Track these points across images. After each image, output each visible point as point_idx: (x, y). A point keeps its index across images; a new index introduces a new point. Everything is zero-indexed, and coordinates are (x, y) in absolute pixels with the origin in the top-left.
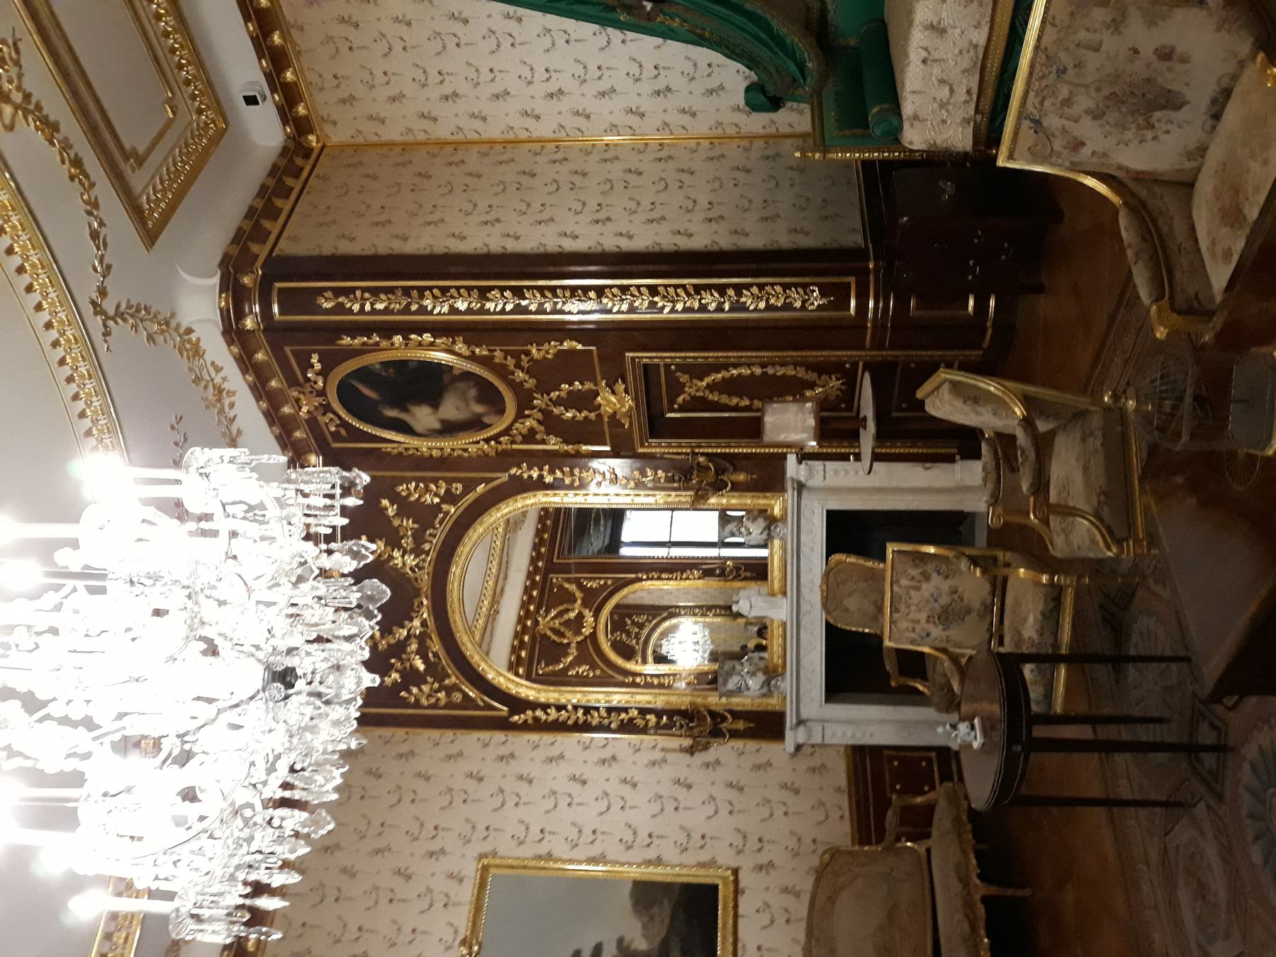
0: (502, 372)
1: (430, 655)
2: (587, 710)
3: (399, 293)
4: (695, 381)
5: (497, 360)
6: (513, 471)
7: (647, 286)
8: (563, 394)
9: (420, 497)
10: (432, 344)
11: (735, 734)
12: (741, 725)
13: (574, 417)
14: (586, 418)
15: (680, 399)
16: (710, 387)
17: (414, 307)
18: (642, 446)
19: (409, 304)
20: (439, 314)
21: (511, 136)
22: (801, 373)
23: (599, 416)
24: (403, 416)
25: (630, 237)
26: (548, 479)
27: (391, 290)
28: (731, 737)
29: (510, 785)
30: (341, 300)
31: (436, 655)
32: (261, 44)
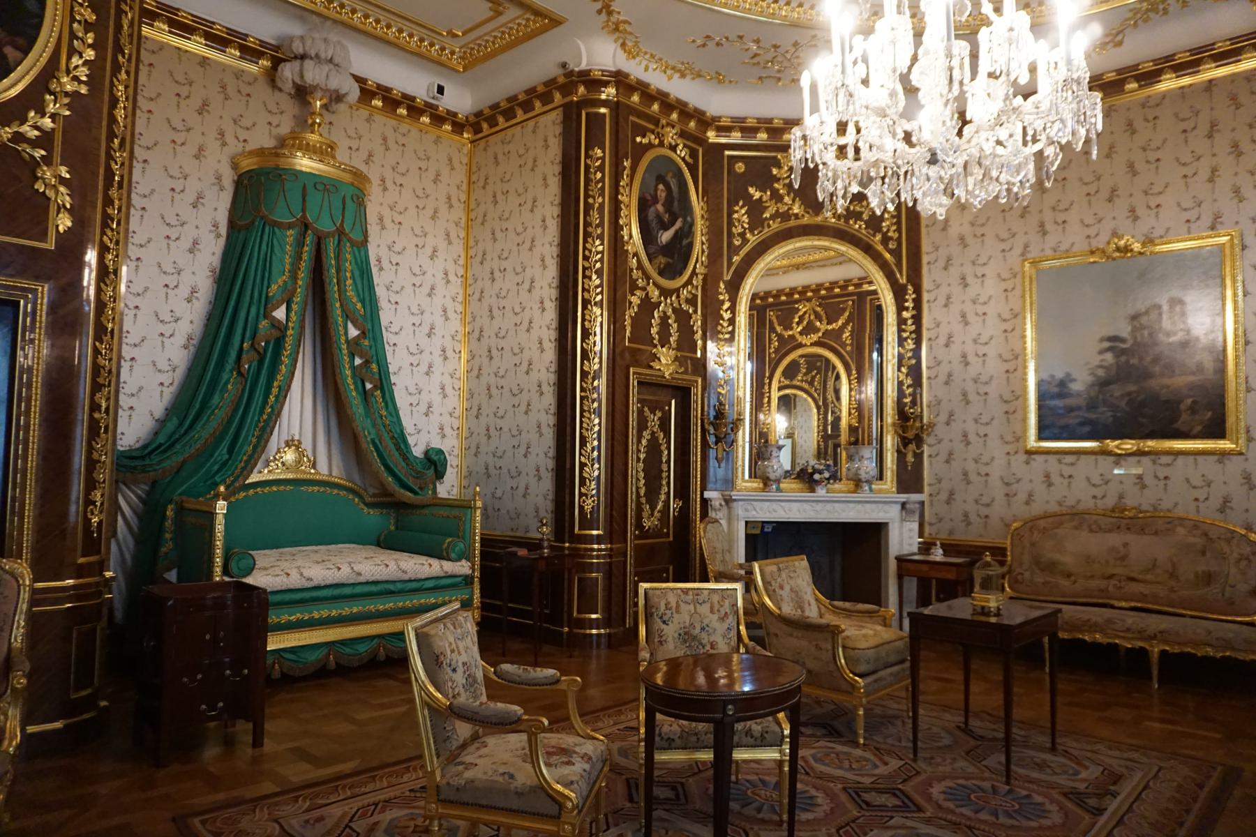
5: (32, 114)
32: (384, 92)
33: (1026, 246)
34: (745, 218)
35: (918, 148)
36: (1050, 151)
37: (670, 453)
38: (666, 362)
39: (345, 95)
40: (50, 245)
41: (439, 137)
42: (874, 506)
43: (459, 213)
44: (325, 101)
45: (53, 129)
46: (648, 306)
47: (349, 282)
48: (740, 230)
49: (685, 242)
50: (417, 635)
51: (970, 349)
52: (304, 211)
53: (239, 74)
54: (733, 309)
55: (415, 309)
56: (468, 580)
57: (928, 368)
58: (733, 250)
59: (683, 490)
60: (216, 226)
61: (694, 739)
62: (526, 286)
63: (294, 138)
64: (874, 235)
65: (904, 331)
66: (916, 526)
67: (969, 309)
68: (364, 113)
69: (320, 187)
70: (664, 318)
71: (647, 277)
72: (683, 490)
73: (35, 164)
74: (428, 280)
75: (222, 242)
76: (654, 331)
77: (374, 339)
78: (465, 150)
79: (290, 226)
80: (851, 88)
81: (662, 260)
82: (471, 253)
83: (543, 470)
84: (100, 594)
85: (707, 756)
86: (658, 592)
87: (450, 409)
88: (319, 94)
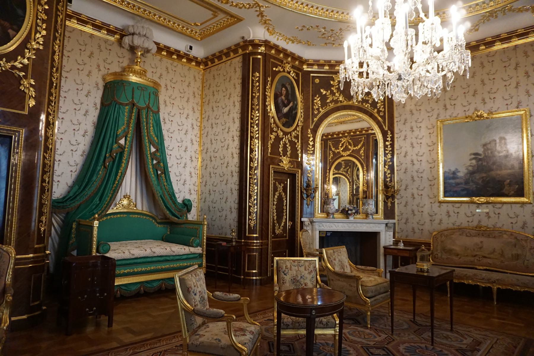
5: (19, 57)
20: (53, 45)
32: (167, 49)
33: (438, 115)
34: (319, 102)
35: (393, 73)
36: (449, 75)
37: (287, 202)
38: (285, 163)
39: (150, 50)
40: (26, 112)
41: (190, 67)
42: (374, 225)
43: (198, 99)
44: (142, 52)
45: (28, 64)
46: (278, 139)
47: (152, 128)
48: (317, 107)
49: (294, 112)
50: (180, 279)
51: (415, 158)
52: (133, 98)
53: (106, 41)
54: (314, 141)
55: (179, 140)
56: (201, 255)
57: (397, 166)
58: (314, 116)
59: (293, 217)
60: (95, 104)
61: (297, 325)
62: (227, 130)
63: (129, 68)
64: (374, 110)
65: (387, 150)
66: (392, 233)
67: (414, 141)
68: (159, 57)
69: (140, 88)
70: (285, 144)
71: (278, 127)
72: (293, 217)
73: (20, 78)
74: (185, 128)
75: (98, 111)
76: (280, 150)
77: (162, 154)
78: (201, 73)
79: (127, 105)
80: (365, 48)
81: (284, 120)
82: (203, 116)
83: (233, 210)
84: (44, 260)
85: (303, 332)
86: (282, 261)
87: (194, 182)
88: (140, 49)
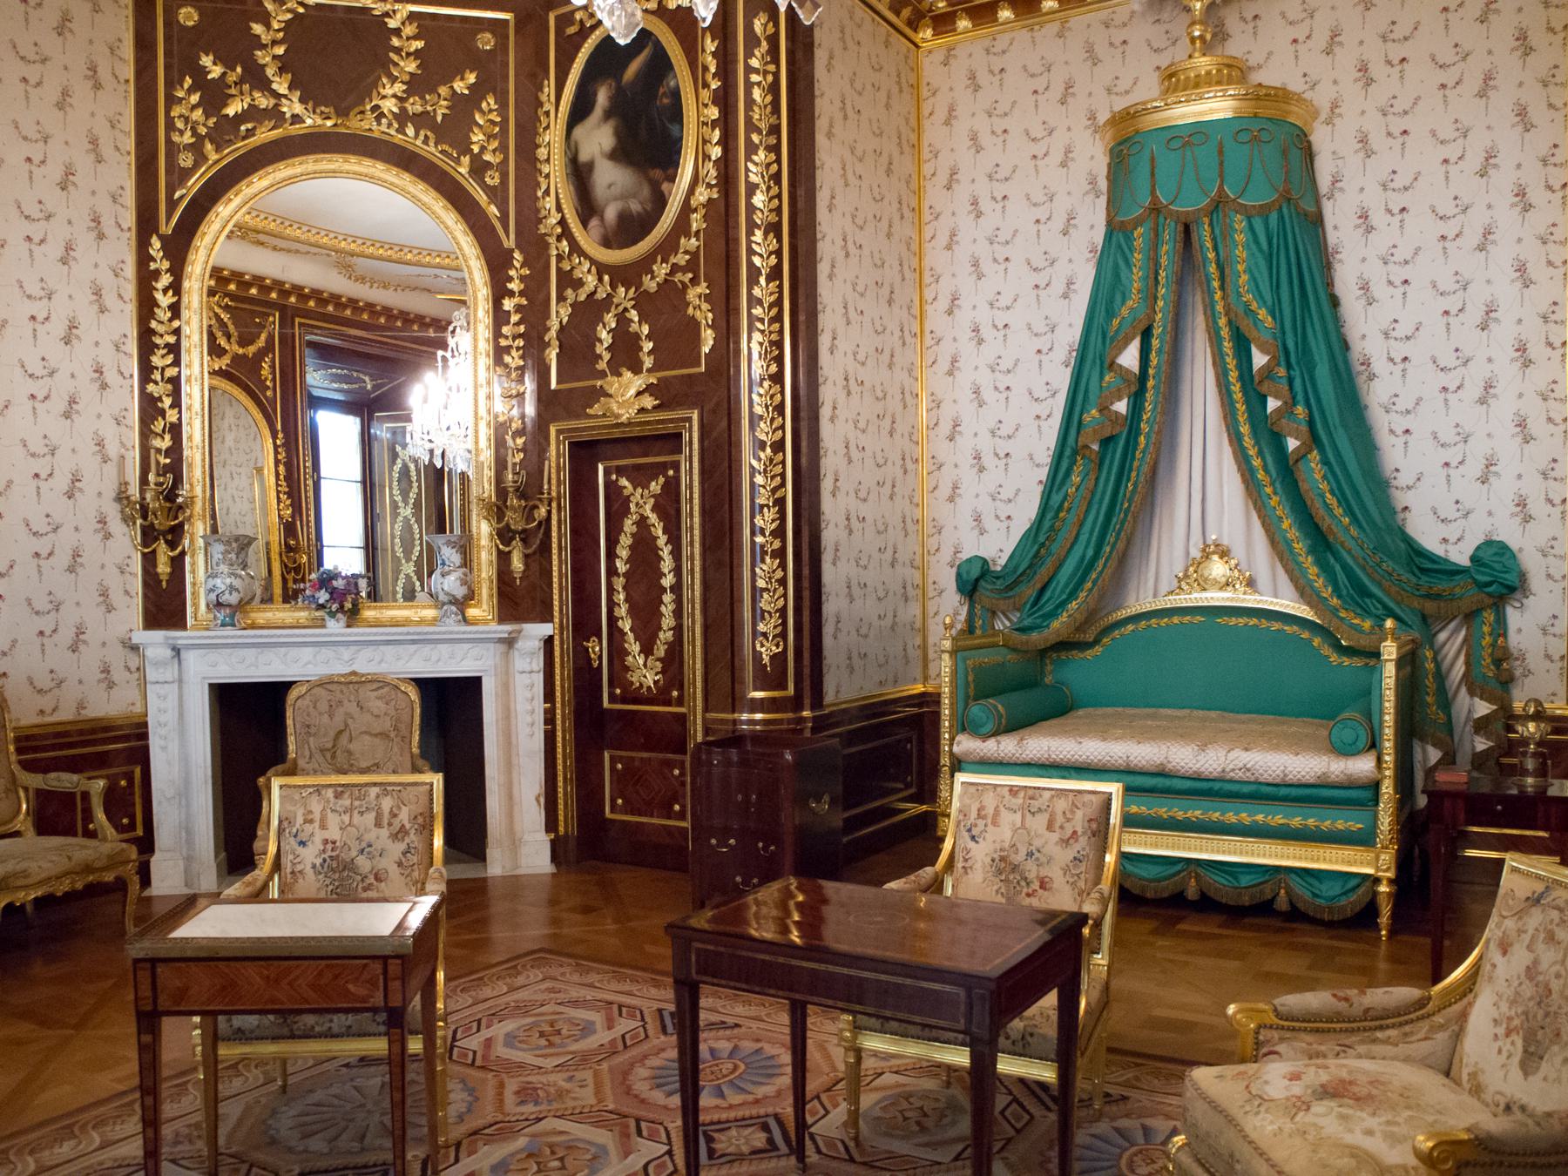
0: (667, 247)
1: (250, 126)
2: (175, 349)
3: (773, 120)
4: (652, 501)
5: (683, 240)
6: (517, 255)
7: (783, 439)
8: (634, 327)
9: (480, 127)
10: (707, 157)
11: (149, 560)
12: (163, 568)
13: (600, 341)
14: (600, 357)
15: (624, 482)
16: (642, 522)
17: (755, 138)
18: (559, 432)
19: (759, 132)
20: (747, 170)
21: (927, 279)
22: (666, 636)
23: (603, 375)
24: (598, 111)
25: (832, 420)
26: (508, 304)
27: (776, 109)
28: (144, 555)
29: (58, 233)
30: (764, 43)
31: (250, 133)
47: (1245, 277)
79: (1138, 222)
87: (1543, 463)
